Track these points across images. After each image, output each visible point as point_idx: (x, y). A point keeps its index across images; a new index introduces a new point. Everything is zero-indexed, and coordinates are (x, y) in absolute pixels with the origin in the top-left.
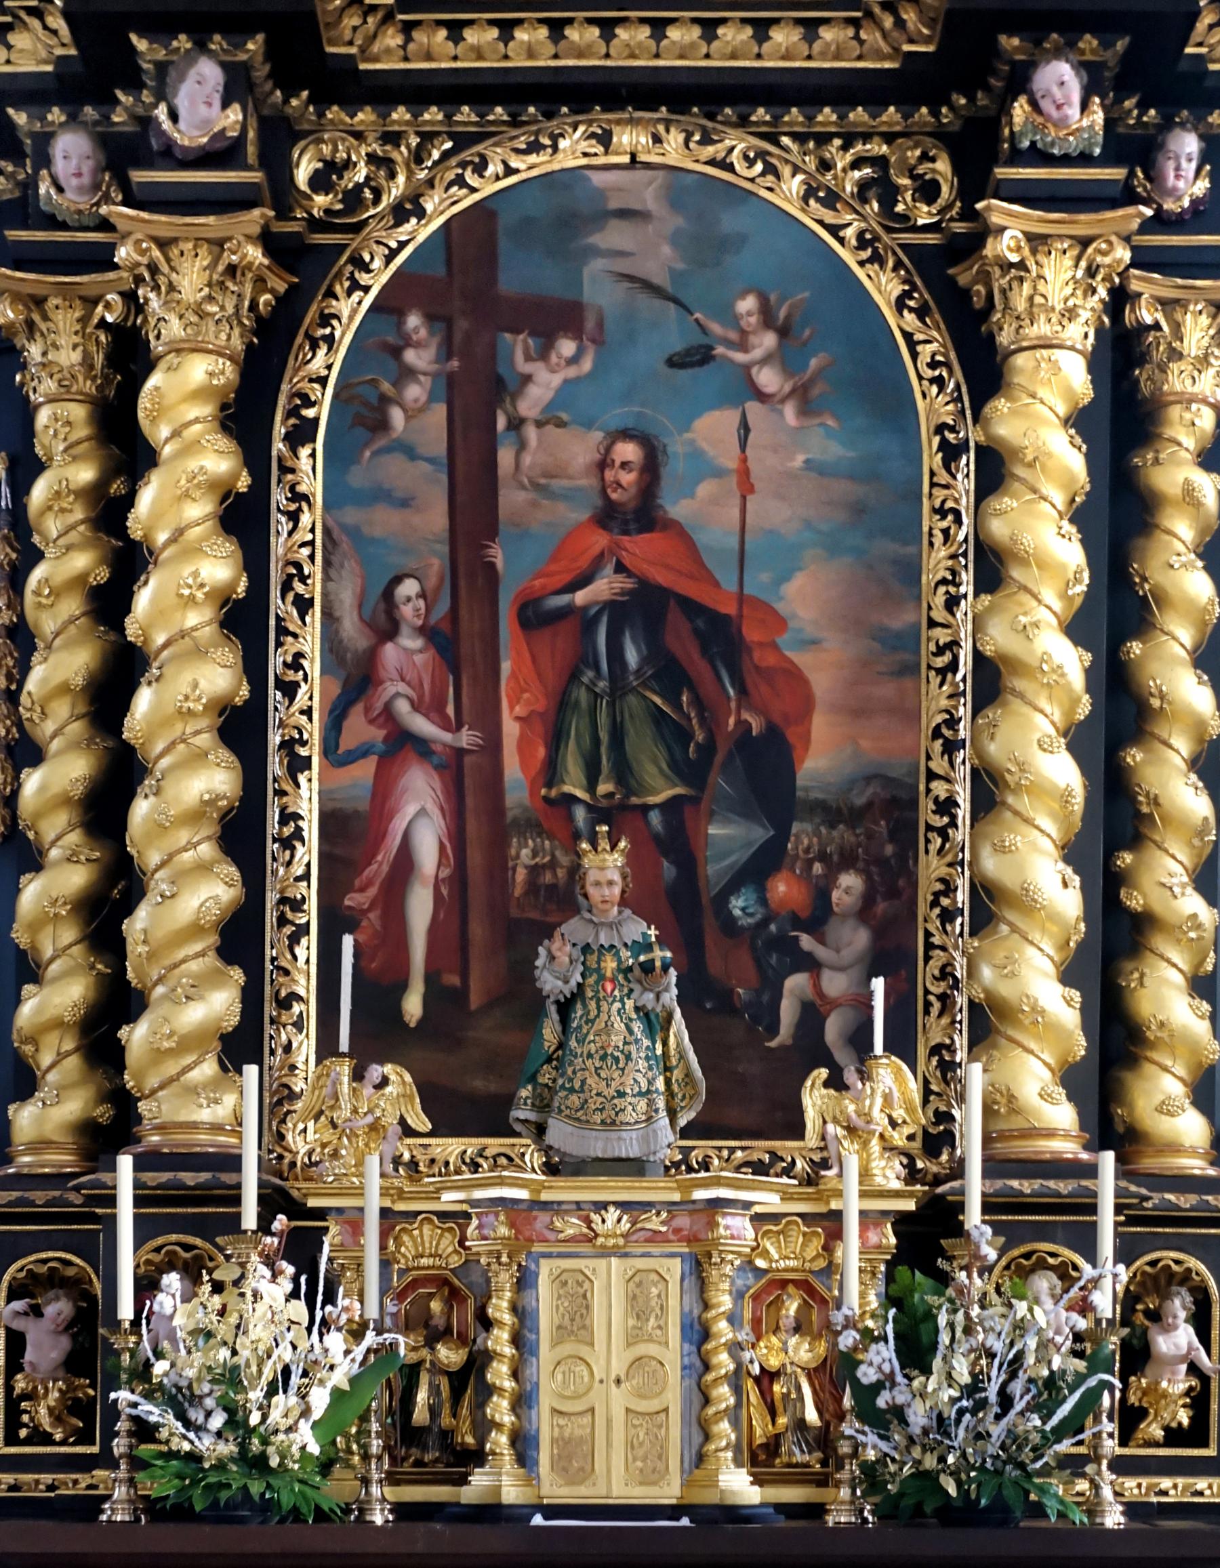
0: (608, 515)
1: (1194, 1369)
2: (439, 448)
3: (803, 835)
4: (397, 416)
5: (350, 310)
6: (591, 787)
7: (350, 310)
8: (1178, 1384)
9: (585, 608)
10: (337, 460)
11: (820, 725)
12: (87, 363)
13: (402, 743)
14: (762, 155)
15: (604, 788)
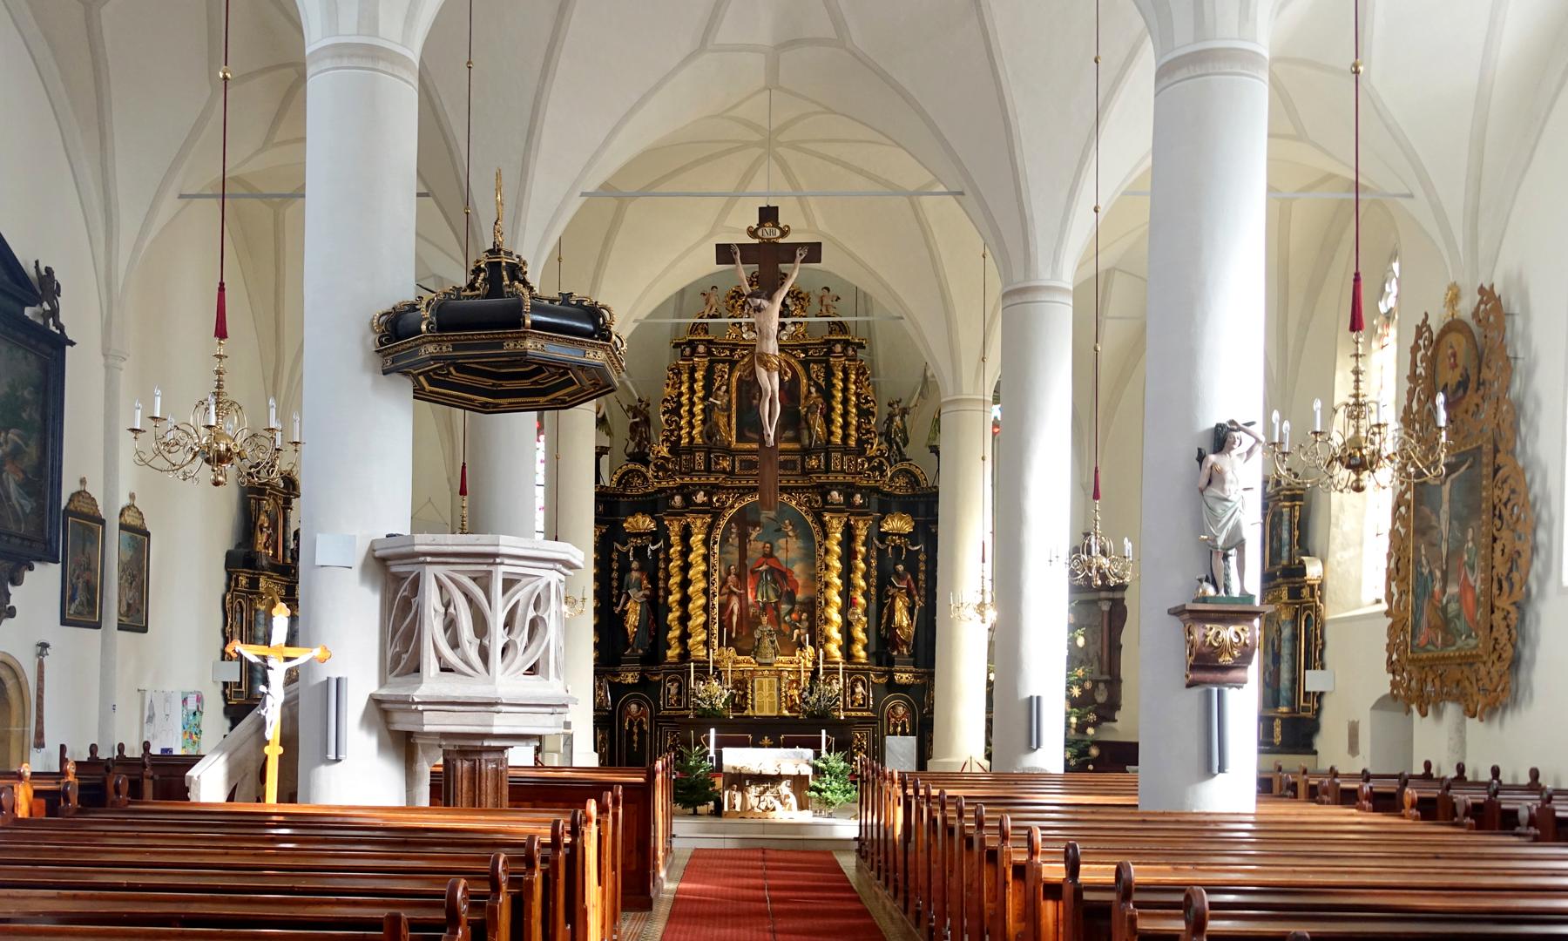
0: (765, 556)
5: (723, 523)
7: (723, 523)
8: (859, 696)
10: (721, 547)
13: (732, 593)
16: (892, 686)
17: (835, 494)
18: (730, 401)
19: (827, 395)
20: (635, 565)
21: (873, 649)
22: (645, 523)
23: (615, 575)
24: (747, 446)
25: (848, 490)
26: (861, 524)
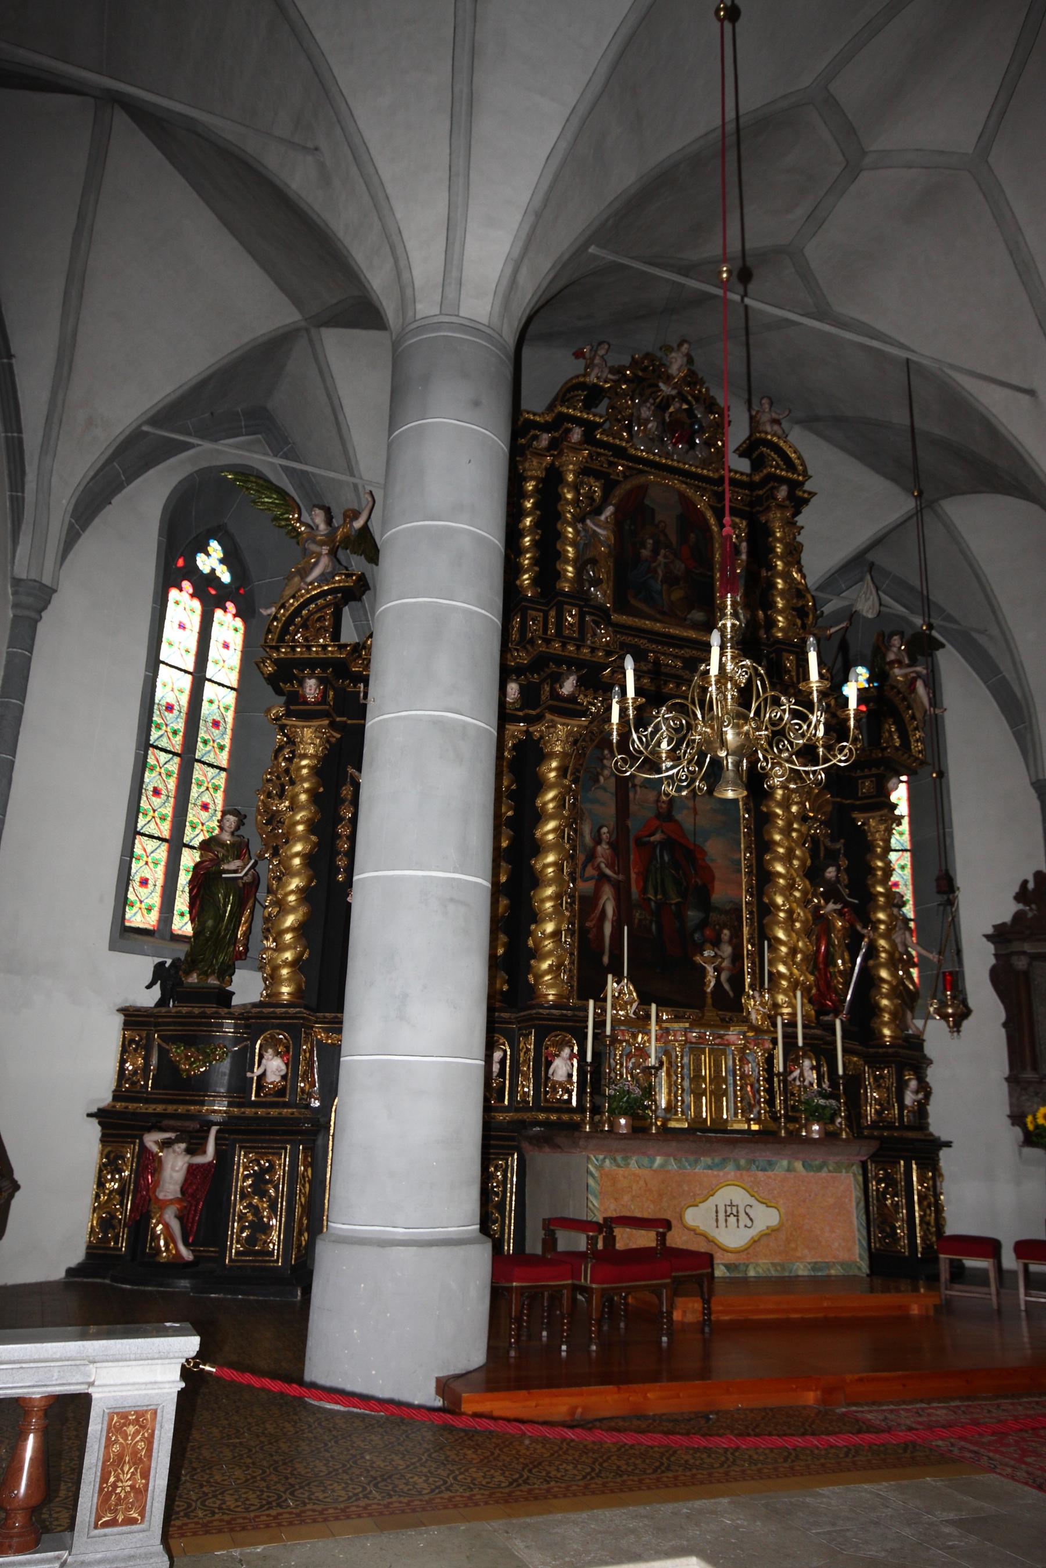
0: (658, 816)
2: (613, 790)
3: (714, 917)
4: (602, 779)
6: (656, 896)
9: (653, 842)
11: (717, 885)
13: (602, 877)
15: (659, 897)
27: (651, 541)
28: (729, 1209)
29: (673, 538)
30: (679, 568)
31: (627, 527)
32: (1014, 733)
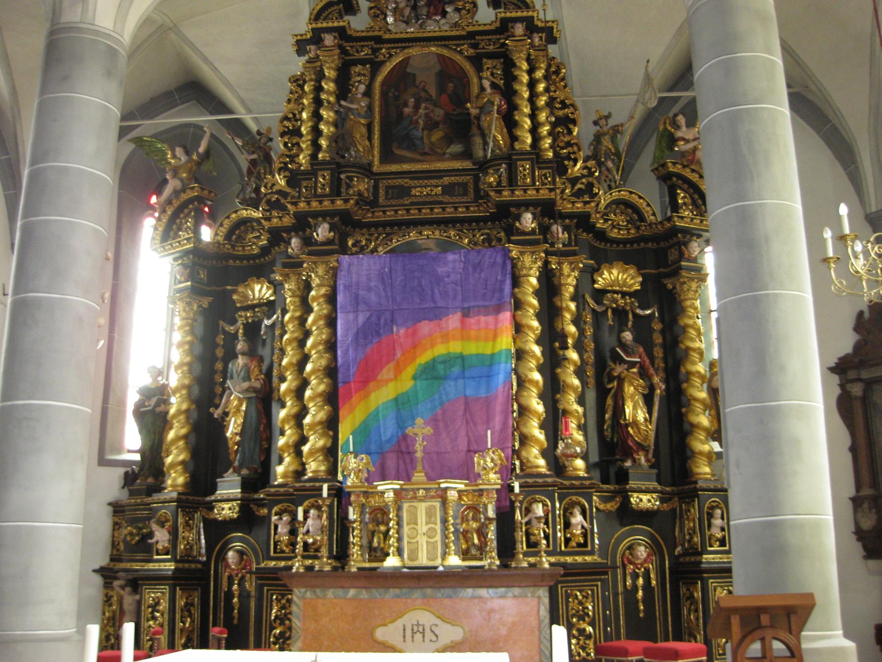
1: (583, 527)
12: (299, 289)
14: (458, 235)
16: (627, 515)
17: (528, 216)
18: (370, 108)
19: (508, 93)
20: (240, 346)
21: (594, 458)
22: (260, 291)
23: (219, 366)
24: (394, 168)
25: (547, 211)
26: (566, 269)
27: (413, 100)
28: (415, 629)
29: (433, 92)
30: (438, 114)
31: (391, 95)
32: (847, 174)
